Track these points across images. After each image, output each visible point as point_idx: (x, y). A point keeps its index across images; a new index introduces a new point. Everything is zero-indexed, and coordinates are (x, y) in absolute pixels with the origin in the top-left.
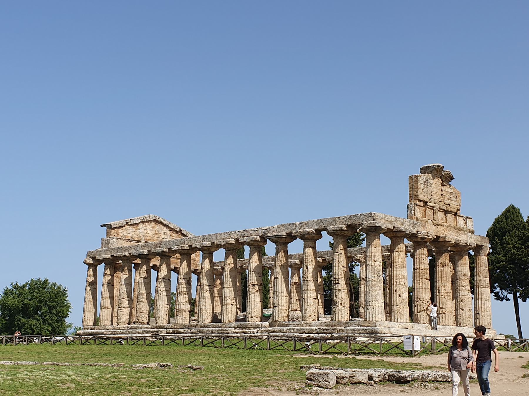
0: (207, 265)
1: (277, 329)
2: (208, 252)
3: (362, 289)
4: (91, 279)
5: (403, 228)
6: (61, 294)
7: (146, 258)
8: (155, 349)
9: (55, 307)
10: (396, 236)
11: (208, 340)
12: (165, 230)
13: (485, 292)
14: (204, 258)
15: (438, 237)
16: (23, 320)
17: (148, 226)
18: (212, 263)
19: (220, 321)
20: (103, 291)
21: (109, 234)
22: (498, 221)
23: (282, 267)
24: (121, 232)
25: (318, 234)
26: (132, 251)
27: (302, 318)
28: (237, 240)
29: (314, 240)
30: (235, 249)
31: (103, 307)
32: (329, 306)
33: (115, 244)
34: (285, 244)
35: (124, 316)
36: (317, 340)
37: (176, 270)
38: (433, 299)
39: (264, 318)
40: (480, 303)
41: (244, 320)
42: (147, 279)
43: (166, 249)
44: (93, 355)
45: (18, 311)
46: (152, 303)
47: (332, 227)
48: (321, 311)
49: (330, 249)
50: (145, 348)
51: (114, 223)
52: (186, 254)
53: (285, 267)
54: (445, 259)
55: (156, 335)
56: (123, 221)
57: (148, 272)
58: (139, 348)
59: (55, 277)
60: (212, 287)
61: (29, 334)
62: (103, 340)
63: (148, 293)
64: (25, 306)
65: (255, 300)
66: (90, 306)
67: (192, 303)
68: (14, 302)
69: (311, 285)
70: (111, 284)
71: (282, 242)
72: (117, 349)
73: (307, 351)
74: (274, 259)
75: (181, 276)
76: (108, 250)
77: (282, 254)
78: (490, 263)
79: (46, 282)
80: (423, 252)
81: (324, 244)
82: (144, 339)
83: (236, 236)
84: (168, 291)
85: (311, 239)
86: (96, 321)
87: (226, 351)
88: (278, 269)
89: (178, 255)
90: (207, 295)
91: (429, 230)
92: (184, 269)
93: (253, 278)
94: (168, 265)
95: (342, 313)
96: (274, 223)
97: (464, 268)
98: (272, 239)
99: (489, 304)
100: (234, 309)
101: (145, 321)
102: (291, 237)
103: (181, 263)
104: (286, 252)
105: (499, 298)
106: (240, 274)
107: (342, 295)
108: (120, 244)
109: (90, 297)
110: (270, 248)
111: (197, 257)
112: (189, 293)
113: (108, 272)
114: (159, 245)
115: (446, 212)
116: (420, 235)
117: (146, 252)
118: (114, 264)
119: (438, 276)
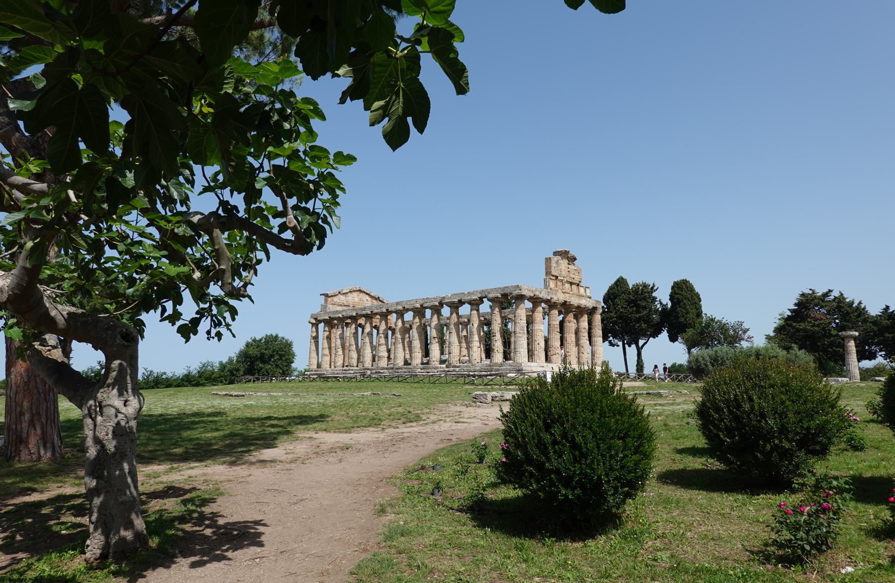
0: (400, 323)
1: (451, 369)
2: (401, 314)
3: (512, 340)
4: (314, 334)
5: (541, 296)
6: (288, 345)
7: (354, 319)
8: (365, 384)
9: (284, 356)
10: (536, 301)
11: (402, 377)
12: (368, 297)
13: (598, 339)
14: (397, 319)
15: (566, 302)
16: (261, 365)
17: (355, 294)
18: (403, 322)
19: (410, 364)
20: (323, 342)
21: (326, 301)
22: (611, 288)
23: (455, 324)
24: (336, 299)
25: (481, 300)
26: (344, 314)
27: (470, 361)
28: (422, 306)
29: (478, 305)
30: (419, 312)
31: (323, 355)
32: (489, 352)
33: (331, 308)
34: (457, 308)
35: (340, 361)
36: (480, 376)
37: (376, 327)
38: (562, 344)
39: (442, 362)
40: (595, 348)
41: (427, 363)
42: (356, 333)
43: (369, 312)
44: (321, 389)
45: (256, 358)
46: (359, 351)
47: (491, 296)
48: (483, 356)
49: (489, 310)
50: (357, 384)
51: (330, 293)
52: (385, 316)
53: (457, 325)
54: (571, 317)
55: (363, 375)
56: (336, 291)
57: (356, 329)
58: (353, 384)
59: (283, 333)
60: (403, 339)
61: (267, 376)
62: (325, 378)
63: (357, 344)
64: (263, 355)
65: (435, 349)
66: (314, 354)
67: (389, 351)
68: (253, 352)
69: (476, 338)
70: (329, 338)
71: (455, 306)
72: (337, 384)
73: (473, 384)
74: (448, 318)
75: (381, 332)
76: (326, 313)
77: (454, 315)
78: (603, 320)
79: (277, 336)
80: (555, 312)
81: (485, 307)
82: (355, 377)
83: (421, 302)
84: (371, 343)
85: (475, 304)
86: (319, 366)
87: (416, 385)
88: (452, 326)
89: (378, 317)
90: (400, 346)
91: (559, 297)
92: (383, 327)
93: (432, 333)
94: (371, 324)
95: (498, 357)
96: (449, 290)
97: (584, 324)
98: (448, 304)
99: (601, 349)
100: (420, 355)
101: (355, 365)
102: (461, 303)
103: (381, 322)
104: (457, 314)
105: (611, 344)
106: (423, 330)
107: (498, 344)
108: (335, 308)
109: (314, 348)
110: (446, 311)
111: (393, 318)
112: (387, 345)
113: (327, 329)
114: (364, 309)
115: (571, 284)
116: (553, 301)
117: (354, 314)
118: (330, 323)
119: (566, 329)
